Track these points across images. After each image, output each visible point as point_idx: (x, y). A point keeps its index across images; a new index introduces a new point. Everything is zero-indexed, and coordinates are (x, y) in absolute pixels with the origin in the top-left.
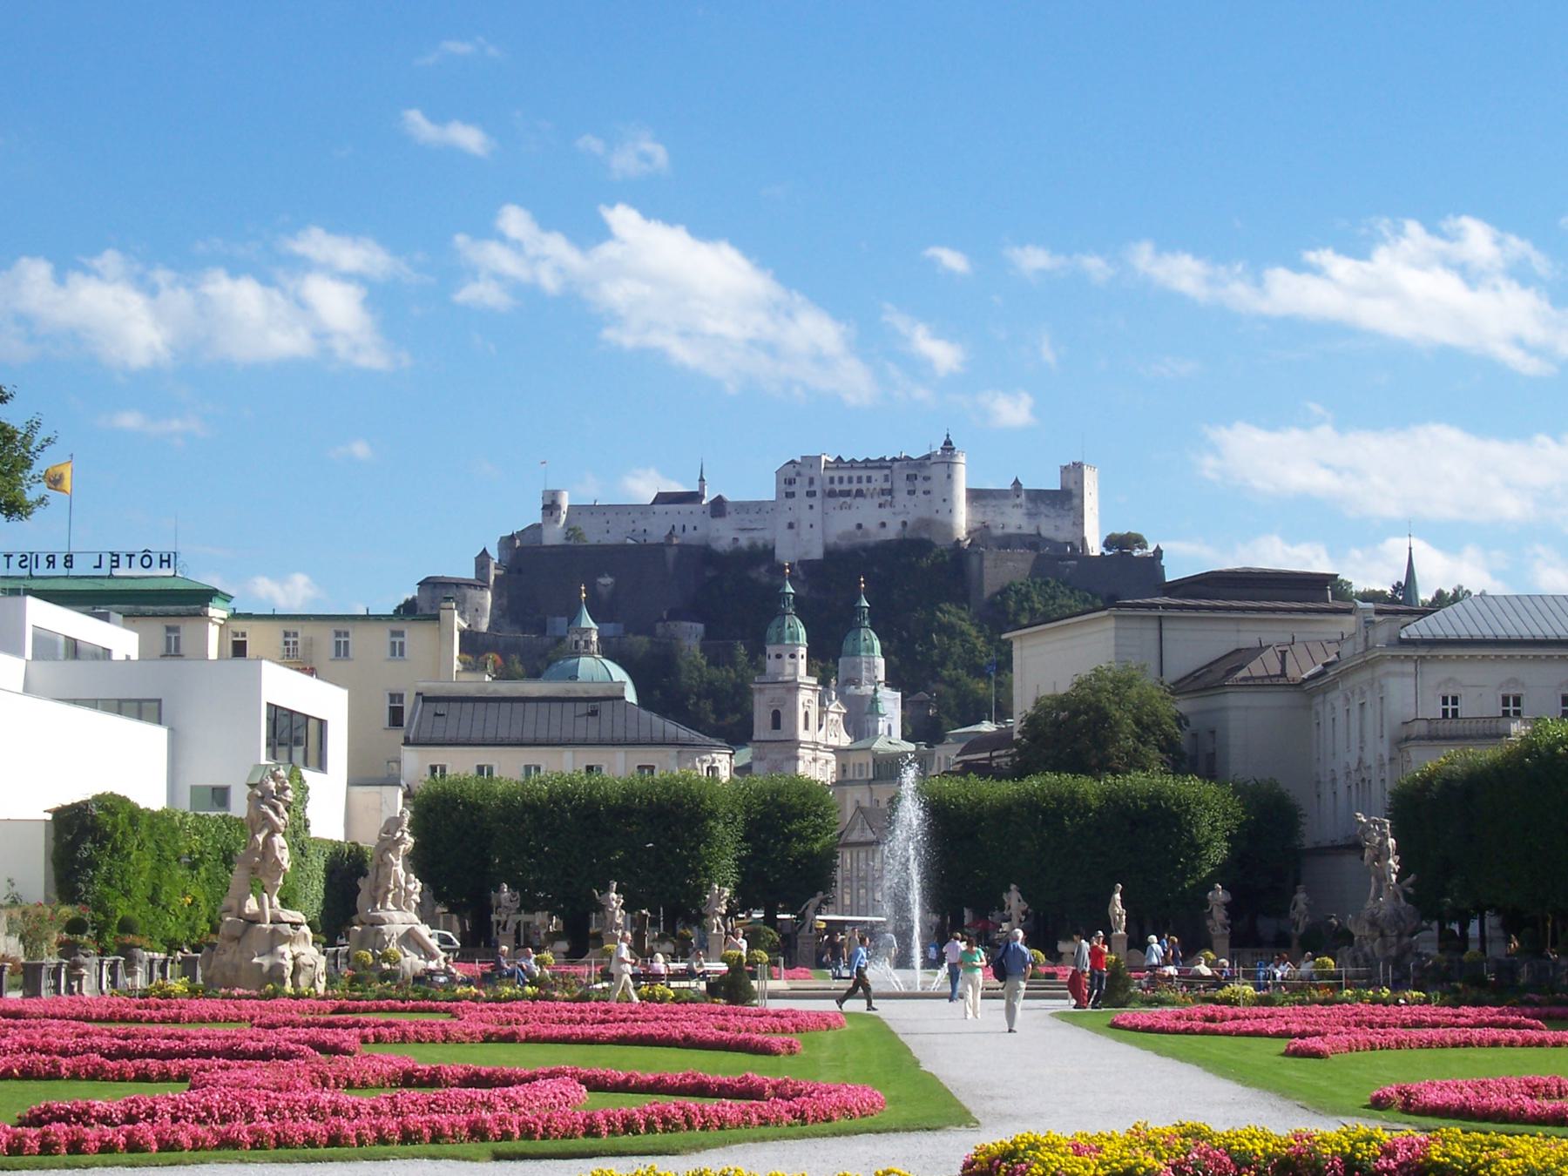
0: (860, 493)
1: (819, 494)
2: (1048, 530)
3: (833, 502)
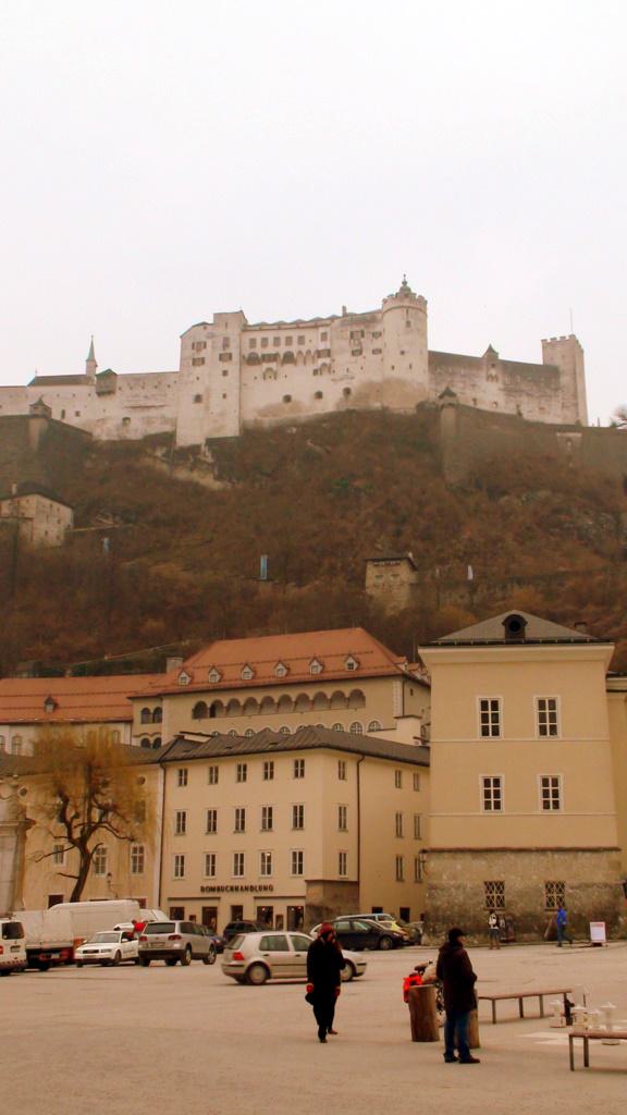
0: (289, 358)
1: (236, 358)
2: (531, 411)
3: (258, 370)
